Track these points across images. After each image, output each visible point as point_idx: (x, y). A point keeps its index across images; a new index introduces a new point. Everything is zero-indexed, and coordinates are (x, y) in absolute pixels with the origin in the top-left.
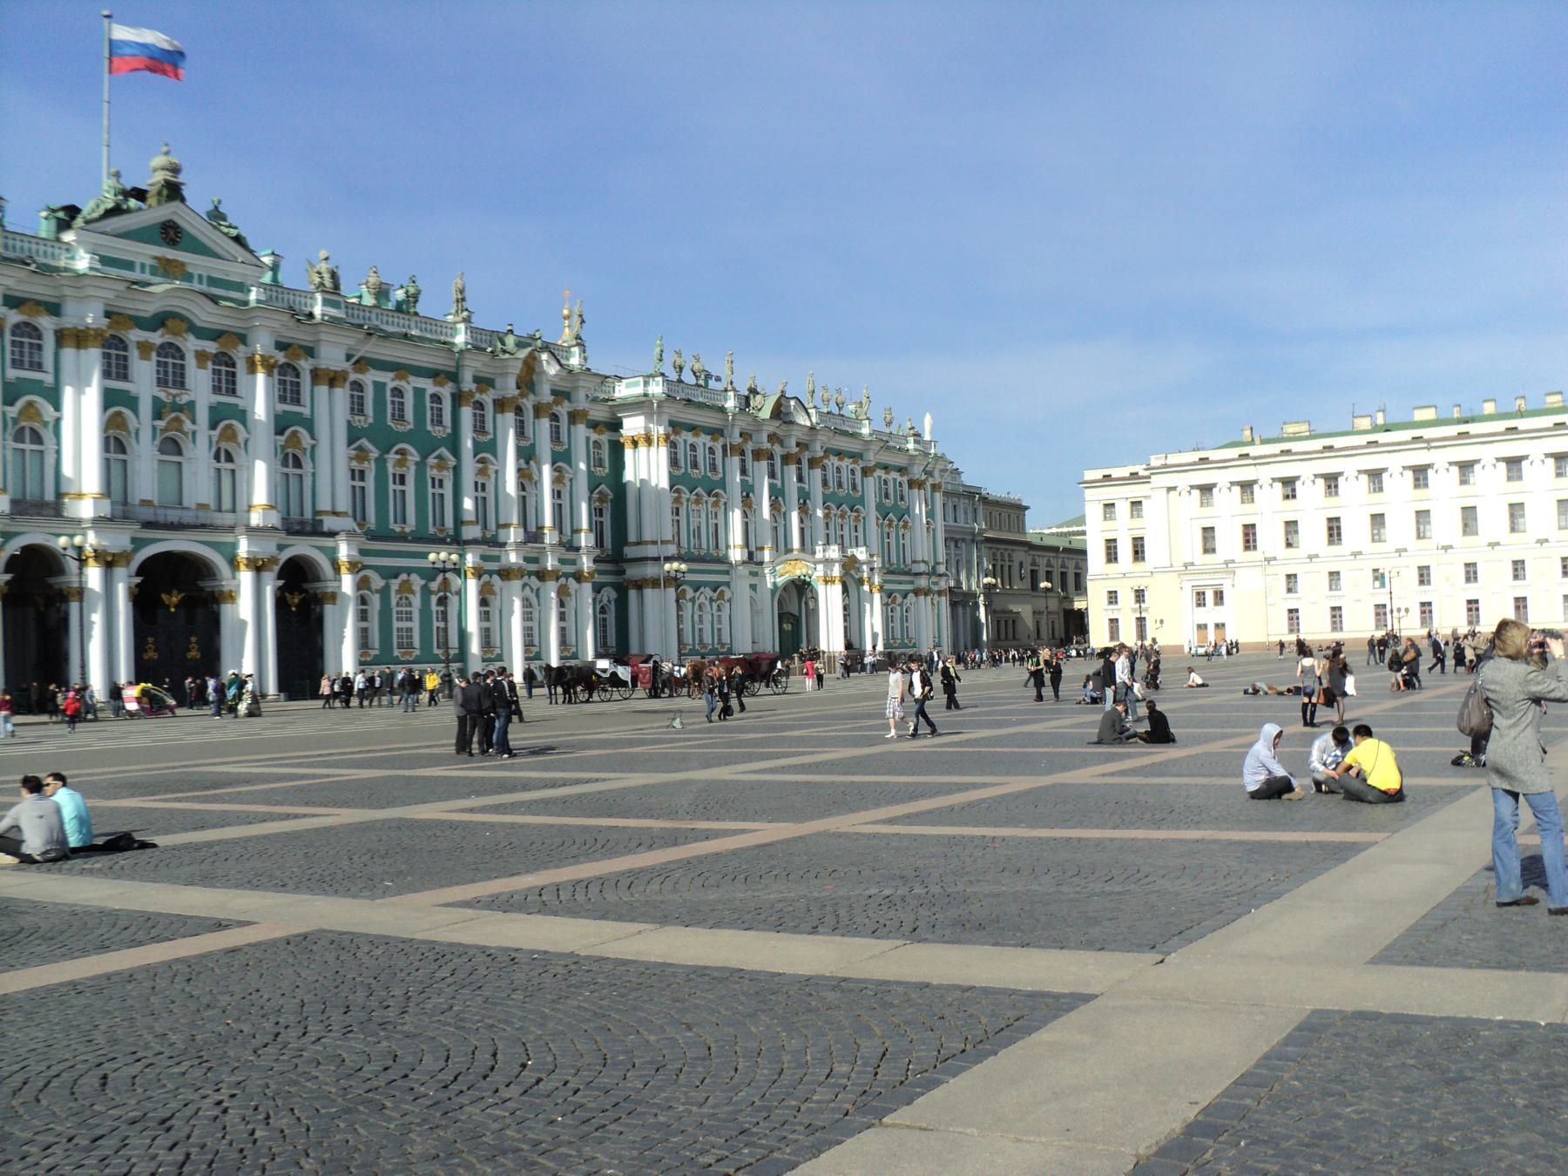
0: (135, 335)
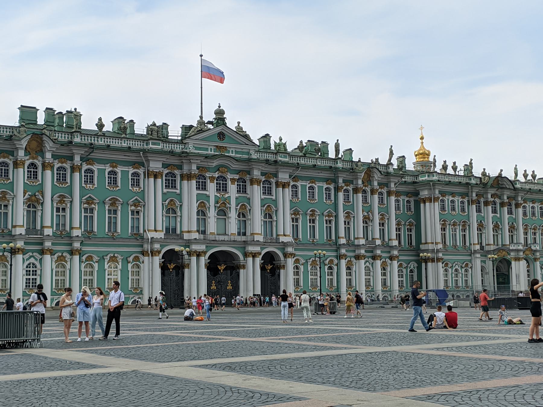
0: (208, 175)
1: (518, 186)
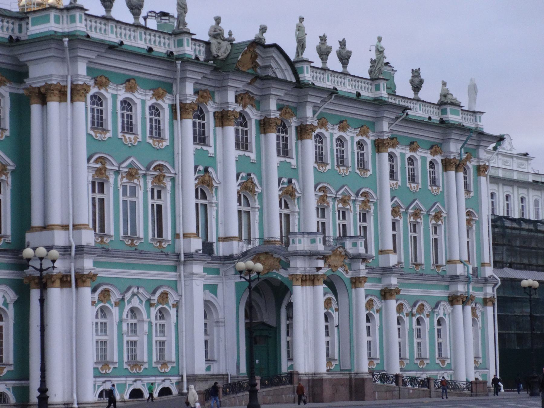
1: (307, 76)
